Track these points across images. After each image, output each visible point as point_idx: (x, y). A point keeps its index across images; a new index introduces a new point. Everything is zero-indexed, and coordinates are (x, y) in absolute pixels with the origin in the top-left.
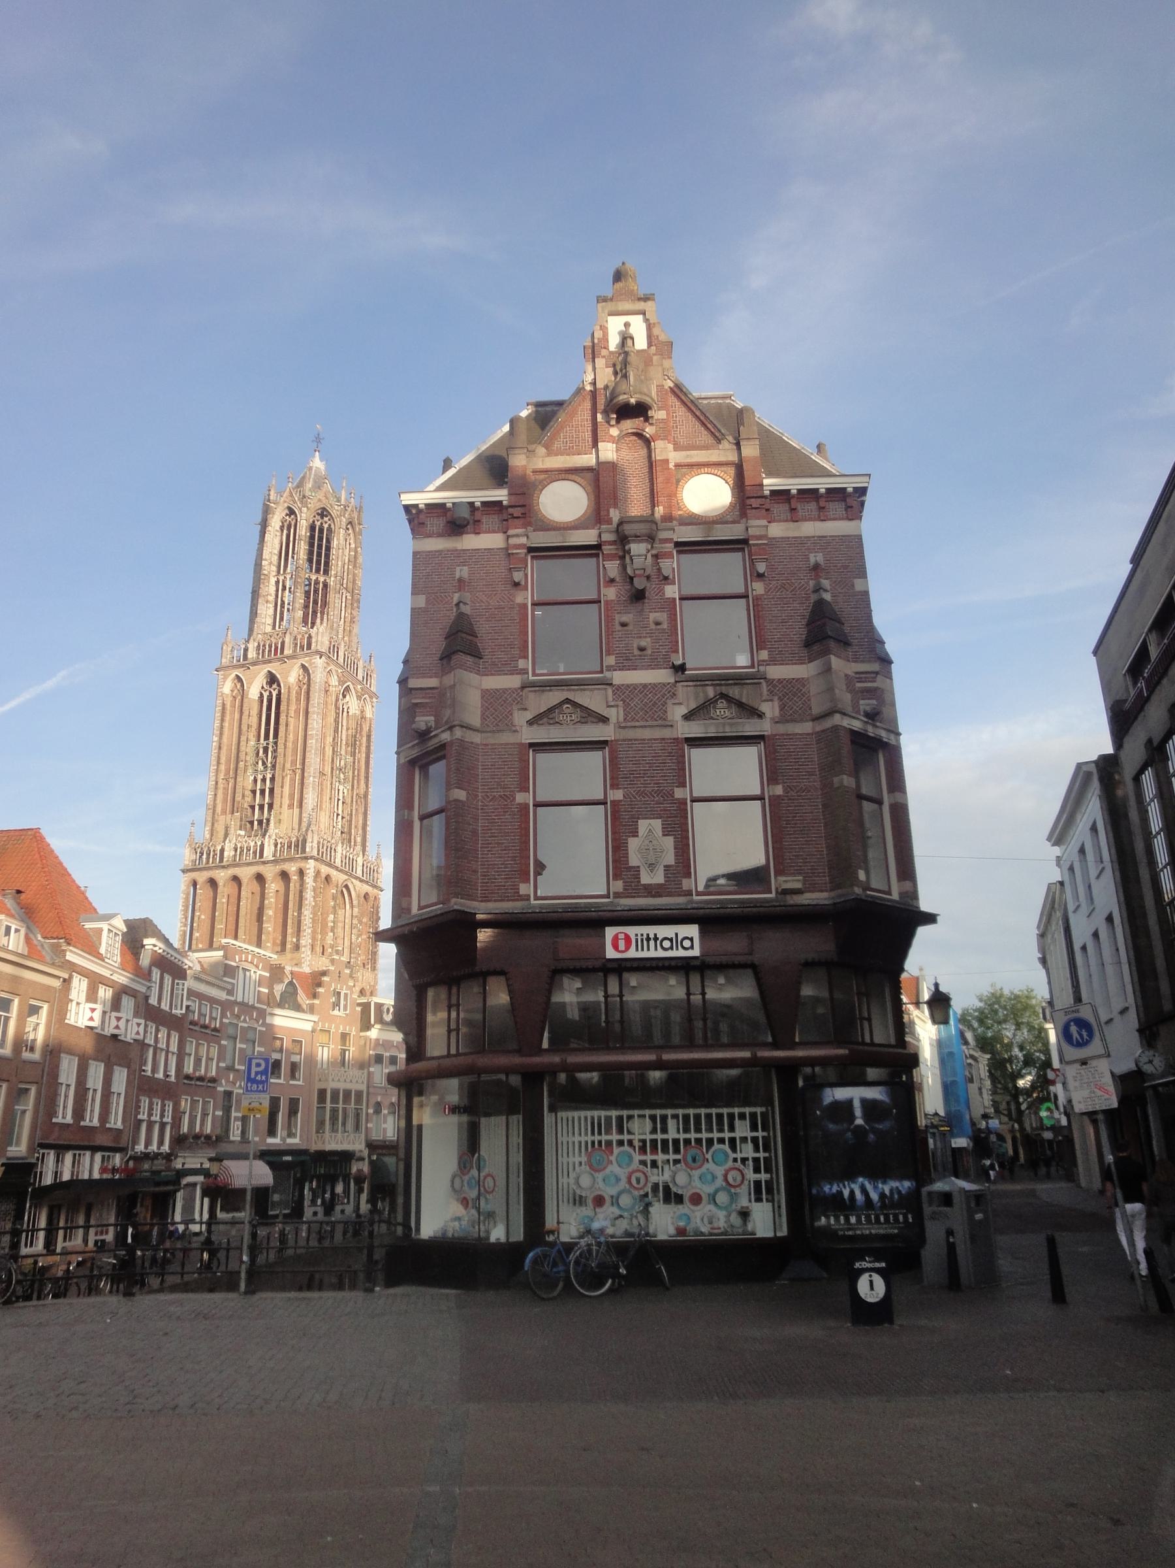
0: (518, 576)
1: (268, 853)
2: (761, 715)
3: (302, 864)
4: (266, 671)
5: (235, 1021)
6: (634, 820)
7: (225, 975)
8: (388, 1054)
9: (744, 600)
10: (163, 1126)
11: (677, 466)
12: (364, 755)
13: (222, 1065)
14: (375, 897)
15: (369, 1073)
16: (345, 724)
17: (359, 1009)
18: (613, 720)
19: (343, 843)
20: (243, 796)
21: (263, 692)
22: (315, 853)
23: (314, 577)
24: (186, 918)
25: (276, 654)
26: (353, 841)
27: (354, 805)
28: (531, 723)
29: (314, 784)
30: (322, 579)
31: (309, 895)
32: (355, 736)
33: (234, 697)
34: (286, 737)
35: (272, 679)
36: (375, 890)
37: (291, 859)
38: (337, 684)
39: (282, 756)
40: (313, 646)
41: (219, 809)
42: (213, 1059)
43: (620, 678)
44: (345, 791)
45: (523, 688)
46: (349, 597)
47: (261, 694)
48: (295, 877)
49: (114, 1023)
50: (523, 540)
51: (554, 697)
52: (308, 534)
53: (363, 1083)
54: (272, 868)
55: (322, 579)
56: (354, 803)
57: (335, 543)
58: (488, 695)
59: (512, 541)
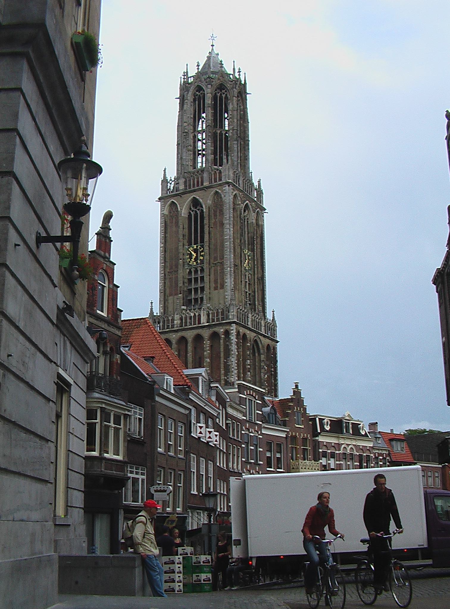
1: (203, 319)
3: (227, 327)
4: (192, 197)
5: (247, 433)
8: (329, 451)
12: (259, 250)
20: (183, 283)
21: (191, 212)
25: (198, 185)
26: (257, 309)
27: (256, 285)
29: (230, 272)
31: (234, 347)
32: (254, 237)
33: (171, 216)
34: (209, 241)
35: (196, 203)
38: (240, 203)
39: (208, 254)
41: (168, 292)
47: (190, 213)
48: (223, 336)
52: (213, 102)
53: (318, 470)
54: (207, 331)
56: (256, 283)
57: (230, 107)
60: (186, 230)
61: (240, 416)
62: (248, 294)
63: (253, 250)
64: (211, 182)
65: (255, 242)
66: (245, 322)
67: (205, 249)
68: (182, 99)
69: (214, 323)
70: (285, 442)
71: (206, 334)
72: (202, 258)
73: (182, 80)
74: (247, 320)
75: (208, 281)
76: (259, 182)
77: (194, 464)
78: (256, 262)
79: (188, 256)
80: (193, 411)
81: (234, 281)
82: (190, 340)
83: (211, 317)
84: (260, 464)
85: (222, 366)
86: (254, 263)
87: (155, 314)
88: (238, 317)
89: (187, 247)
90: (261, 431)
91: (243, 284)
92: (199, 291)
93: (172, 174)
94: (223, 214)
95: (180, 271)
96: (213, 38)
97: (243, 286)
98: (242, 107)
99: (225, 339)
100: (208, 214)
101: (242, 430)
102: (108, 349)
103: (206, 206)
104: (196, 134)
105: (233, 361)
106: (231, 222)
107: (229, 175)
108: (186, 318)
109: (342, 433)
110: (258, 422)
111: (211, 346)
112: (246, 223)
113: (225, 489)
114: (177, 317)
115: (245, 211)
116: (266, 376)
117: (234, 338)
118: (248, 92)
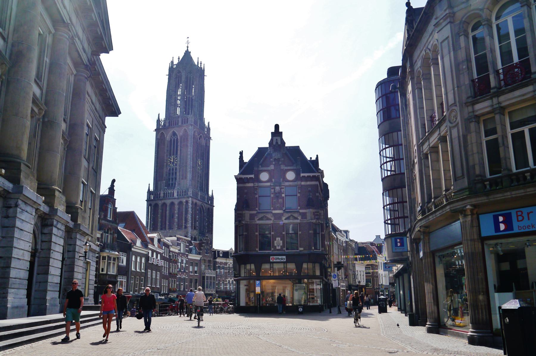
0: (256, 192)
1: (175, 195)
2: (298, 219)
3: (187, 199)
7: (177, 246)
9: (296, 196)
10: (166, 286)
11: (285, 170)
13: (178, 270)
16: (200, 149)
17: (213, 253)
18: (272, 219)
19: (200, 190)
22: (191, 195)
25: (176, 125)
30: (191, 97)
31: (190, 210)
34: (180, 154)
35: (174, 134)
37: (184, 198)
40: (189, 122)
43: (274, 212)
45: (257, 213)
47: (171, 139)
48: (185, 204)
50: (257, 185)
59: (255, 185)
61: (177, 251)
62: (199, 182)
63: (203, 159)
64: (182, 123)
71: (176, 202)
72: (176, 163)
76: (209, 123)
77: (149, 273)
79: (169, 161)
80: (150, 252)
82: (168, 204)
85: (184, 219)
87: (151, 190)
89: (169, 156)
90: (188, 257)
93: (163, 117)
95: (165, 169)
99: (186, 205)
101: (178, 257)
102: (112, 233)
106: (192, 145)
108: (166, 193)
109: (228, 258)
110: (186, 253)
111: (179, 209)
112: (200, 145)
114: (162, 193)
115: (200, 139)
117: (190, 205)
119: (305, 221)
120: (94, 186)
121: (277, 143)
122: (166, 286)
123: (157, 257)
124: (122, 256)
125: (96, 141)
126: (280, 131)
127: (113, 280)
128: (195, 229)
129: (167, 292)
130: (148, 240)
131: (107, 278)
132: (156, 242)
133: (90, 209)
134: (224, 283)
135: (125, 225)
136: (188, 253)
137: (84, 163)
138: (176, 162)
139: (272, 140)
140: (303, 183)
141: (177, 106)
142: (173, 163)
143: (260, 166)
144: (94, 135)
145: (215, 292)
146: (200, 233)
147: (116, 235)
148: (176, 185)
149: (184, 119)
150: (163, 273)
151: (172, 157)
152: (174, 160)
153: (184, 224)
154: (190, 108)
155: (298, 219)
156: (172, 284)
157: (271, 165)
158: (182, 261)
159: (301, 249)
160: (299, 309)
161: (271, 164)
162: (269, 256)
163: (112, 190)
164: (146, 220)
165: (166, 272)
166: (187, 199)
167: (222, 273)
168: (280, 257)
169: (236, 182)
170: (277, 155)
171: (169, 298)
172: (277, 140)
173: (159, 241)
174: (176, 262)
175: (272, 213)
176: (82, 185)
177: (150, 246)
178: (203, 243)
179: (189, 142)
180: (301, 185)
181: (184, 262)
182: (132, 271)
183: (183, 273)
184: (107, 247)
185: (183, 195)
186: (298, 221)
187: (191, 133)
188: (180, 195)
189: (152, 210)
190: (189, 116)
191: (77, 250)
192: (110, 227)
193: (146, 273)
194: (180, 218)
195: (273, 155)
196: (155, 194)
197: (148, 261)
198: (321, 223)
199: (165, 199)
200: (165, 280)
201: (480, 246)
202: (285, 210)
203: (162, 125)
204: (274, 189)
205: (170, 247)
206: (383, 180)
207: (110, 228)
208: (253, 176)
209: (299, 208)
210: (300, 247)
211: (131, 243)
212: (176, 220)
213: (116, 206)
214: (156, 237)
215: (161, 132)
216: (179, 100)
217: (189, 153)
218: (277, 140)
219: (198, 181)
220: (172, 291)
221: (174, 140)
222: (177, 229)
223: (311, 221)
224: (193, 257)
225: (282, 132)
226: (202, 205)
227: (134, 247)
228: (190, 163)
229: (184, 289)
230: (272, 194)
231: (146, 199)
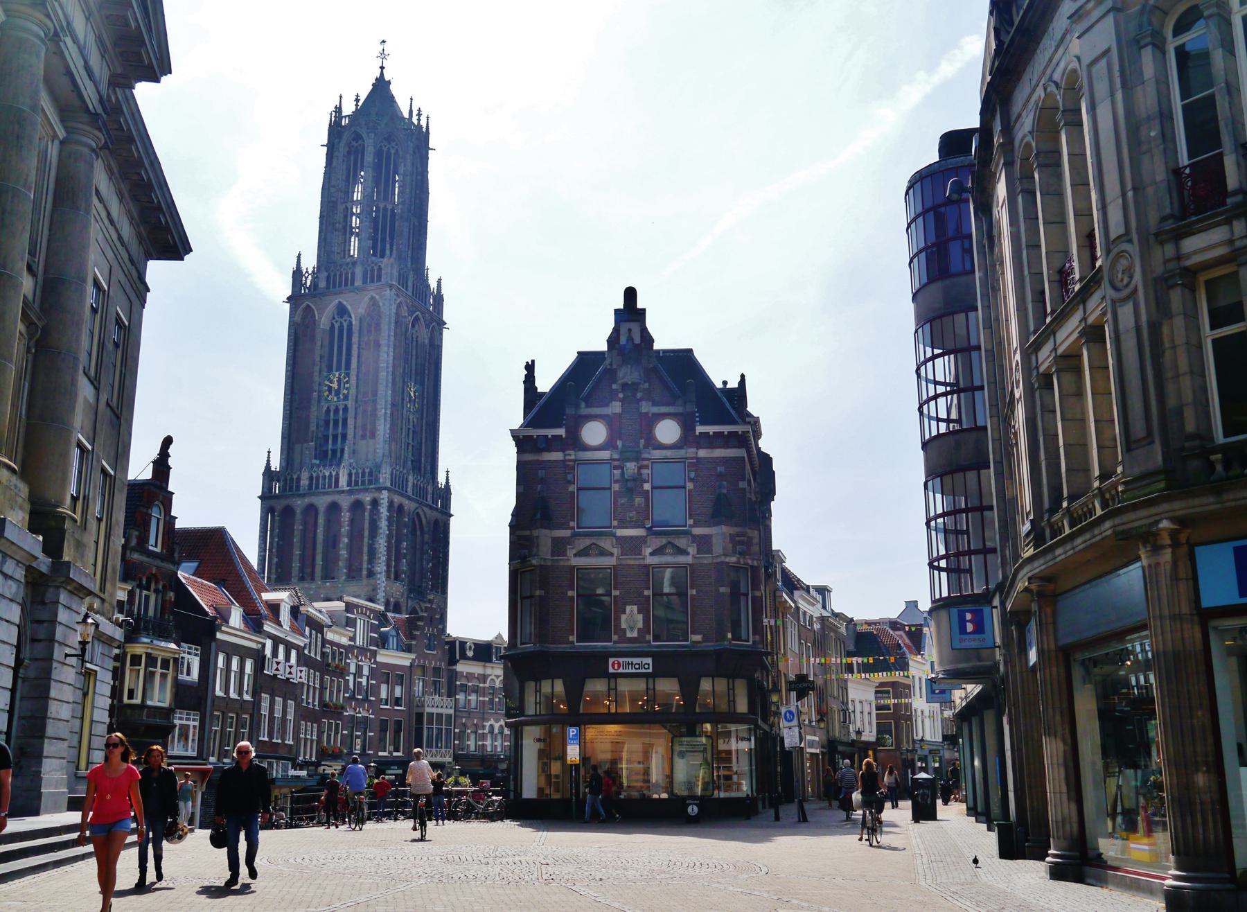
0: (570, 477)
1: (343, 481)
2: (688, 554)
3: (376, 495)
6: (625, 605)
7: (347, 626)
9: (684, 490)
10: (312, 741)
11: (653, 414)
13: (347, 695)
14: (445, 524)
15: (455, 699)
17: (447, 647)
18: (616, 554)
20: (317, 426)
22: (388, 485)
23: (382, 205)
24: (266, 546)
25: (346, 285)
26: (423, 469)
28: (575, 555)
30: (389, 207)
31: (383, 525)
34: (358, 368)
35: (342, 311)
36: (444, 517)
37: (366, 490)
38: (406, 314)
42: (340, 691)
43: (621, 532)
44: (415, 420)
46: (416, 224)
47: (332, 324)
48: (369, 507)
49: (288, 670)
50: (573, 457)
51: (588, 542)
55: (389, 207)
57: (402, 169)
58: (555, 540)
59: (568, 458)
60: (327, 349)
61: (345, 641)
62: (410, 448)
63: (422, 384)
64: (365, 282)
65: (426, 372)
66: (403, 487)
67: (351, 379)
68: (331, 147)
69: (357, 488)
70: (408, 673)
71: (345, 502)
72: (346, 392)
73: (333, 119)
74: (407, 485)
75: (352, 427)
76: (439, 282)
77: (265, 705)
78: (425, 400)
79: (326, 388)
80: (269, 643)
81: (390, 429)
82: (322, 510)
83: (353, 479)
84: (371, 701)
85: (365, 549)
86: (423, 402)
88: (392, 480)
89: (325, 374)
90: (375, 658)
91: (404, 434)
92: (339, 439)
93: (310, 262)
94: (380, 330)
95: (314, 409)
96: (383, 55)
97: (403, 436)
98: (420, 169)
99: (371, 511)
100: (358, 328)
101: (347, 657)
102: (160, 587)
103: (356, 317)
104: (349, 206)
105: (382, 544)
106: (391, 343)
107: (391, 274)
109: (490, 661)
110: (371, 648)
111: (352, 521)
112: (414, 343)
113: (315, 733)
114: (305, 477)
115: (413, 326)
116: (430, 564)
117: (384, 511)
118: (431, 146)
119: (707, 559)
120: (113, 454)
121: (630, 339)
122: (312, 741)
123: (287, 658)
124: (189, 653)
125: (120, 327)
126: (639, 306)
127: (159, 721)
128: (397, 578)
129: (313, 759)
130: (264, 610)
131: (145, 718)
132: (285, 616)
133: (100, 520)
134: (476, 732)
135: (198, 567)
136: (377, 646)
137: (85, 390)
138: (347, 389)
139: (616, 330)
140: (702, 453)
141: (352, 234)
142: (338, 392)
143: (583, 405)
144: (114, 311)
145: (451, 760)
146: (410, 591)
147: (171, 595)
148: (346, 455)
149: (369, 269)
150: (305, 704)
151: (334, 375)
152: (339, 385)
153: (365, 566)
154: (388, 239)
155: (688, 554)
156: (329, 736)
157: (614, 403)
158: (359, 668)
159: (698, 638)
160: (690, 809)
161: (613, 396)
162: (604, 656)
163: (162, 466)
164: (259, 552)
165: (314, 701)
166: (376, 495)
167: (473, 705)
168: (636, 660)
169: (515, 449)
170: (631, 372)
171: (320, 774)
172: (630, 330)
173: (295, 611)
174: (342, 672)
175: (614, 535)
176: (75, 454)
177: (268, 627)
178: (420, 619)
179: (384, 334)
180: (697, 458)
181: (366, 671)
182: (215, 697)
183: (360, 703)
184: (146, 629)
185: (363, 483)
186: (688, 560)
187: (390, 310)
188: (357, 483)
189: (277, 525)
190: (385, 260)
191: (59, 635)
192: (154, 571)
193: (256, 704)
194: (354, 548)
195: (620, 374)
196: (286, 480)
197: (263, 668)
198: (752, 567)
199: (313, 494)
200: (309, 724)
201: (1198, 635)
202: (651, 527)
203: (308, 284)
204: (622, 468)
205: (325, 629)
206: (925, 445)
207: (155, 576)
208: (561, 432)
209: (690, 522)
210: (692, 633)
211: (216, 618)
212: (344, 553)
213: (173, 514)
214: (287, 600)
215: (304, 305)
216: (358, 216)
217: (383, 365)
218: (630, 330)
219: (408, 444)
220: (330, 755)
221: (341, 327)
222: (345, 580)
223: (722, 559)
224: (392, 657)
225: (644, 310)
226: (419, 511)
227: (223, 628)
228: (385, 394)
229: (364, 748)
230: (616, 482)
231: (260, 494)
